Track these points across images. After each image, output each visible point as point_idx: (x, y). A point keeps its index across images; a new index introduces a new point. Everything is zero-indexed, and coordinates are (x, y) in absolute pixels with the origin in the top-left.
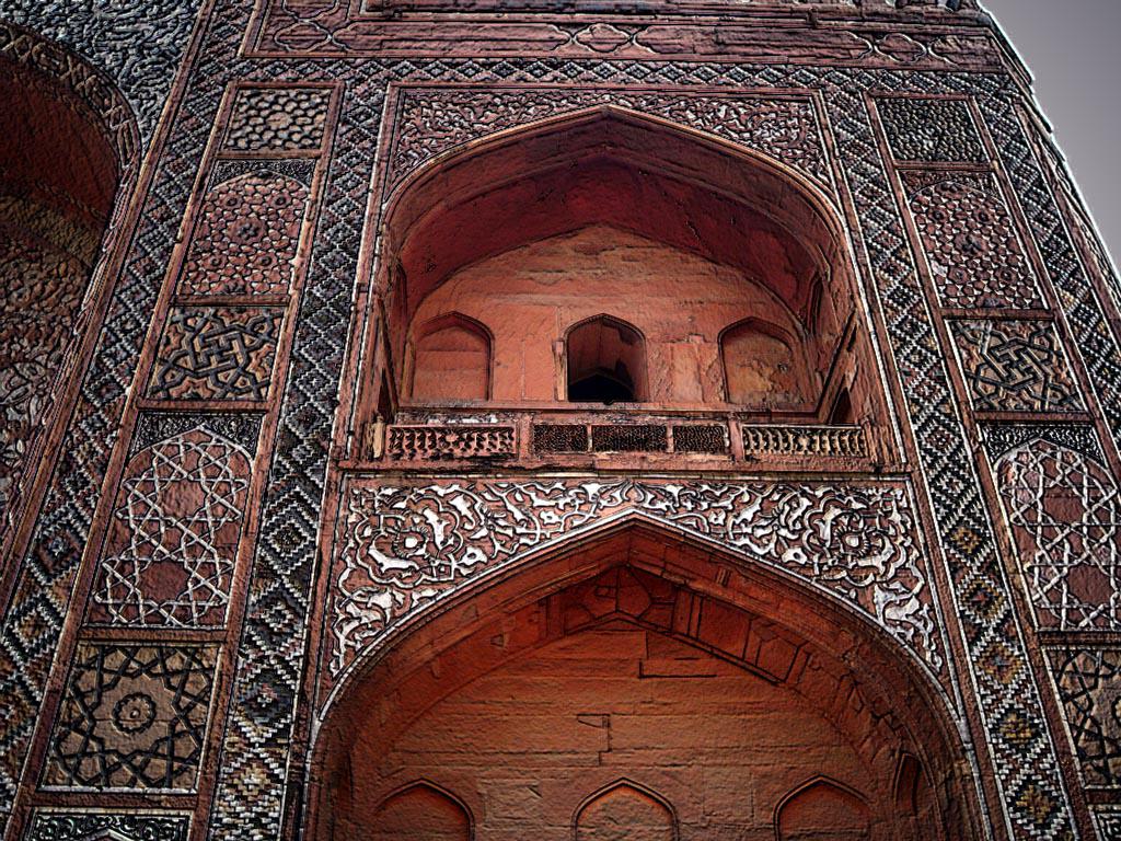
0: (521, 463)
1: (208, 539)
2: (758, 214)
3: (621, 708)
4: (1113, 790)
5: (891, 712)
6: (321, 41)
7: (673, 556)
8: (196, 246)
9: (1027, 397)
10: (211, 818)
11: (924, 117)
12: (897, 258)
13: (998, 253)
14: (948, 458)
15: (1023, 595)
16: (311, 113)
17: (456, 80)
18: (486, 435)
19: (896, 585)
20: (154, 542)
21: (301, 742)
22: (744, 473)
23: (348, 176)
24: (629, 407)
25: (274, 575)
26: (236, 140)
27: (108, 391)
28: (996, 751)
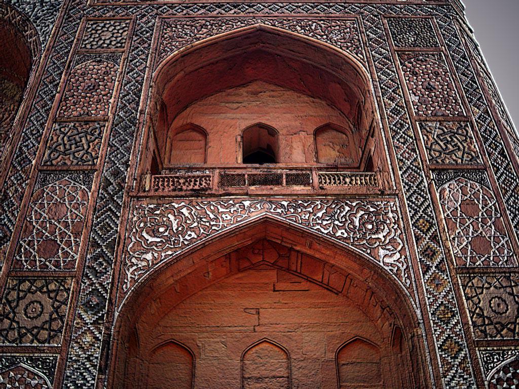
0: (213, 192)
1: (68, 230)
2: (330, 74)
3: (263, 306)
4: (488, 341)
5: (388, 307)
7: (285, 234)
8: (66, 95)
9: (454, 158)
10: (67, 357)
11: (410, 27)
13: (443, 90)
14: (416, 187)
15: (449, 251)
16: (121, 31)
17: (189, 14)
19: (390, 247)
20: (44, 231)
21: (109, 322)
22: (319, 195)
23: (137, 60)
24: (271, 166)
25: (99, 246)
26: (86, 44)
27: (24, 162)
28: (434, 324)
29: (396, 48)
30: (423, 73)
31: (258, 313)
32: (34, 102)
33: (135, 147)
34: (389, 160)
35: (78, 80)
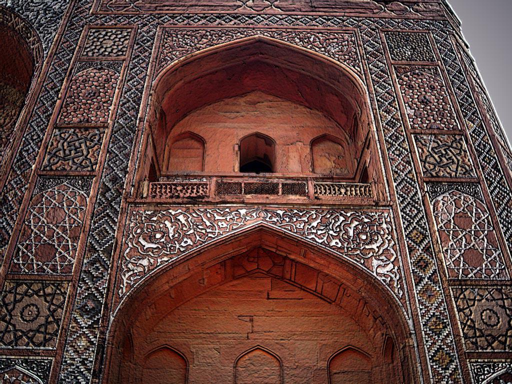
0: (210, 200)
1: (66, 234)
2: (328, 86)
4: (478, 352)
5: (381, 316)
6: (128, 7)
7: (280, 243)
8: (67, 101)
9: (449, 171)
11: (407, 41)
12: (391, 106)
13: (438, 104)
14: (411, 199)
15: (442, 263)
16: (122, 40)
17: (189, 24)
18: (195, 187)
19: (383, 257)
20: (42, 235)
22: (314, 205)
23: (137, 68)
24: (267, 175)
25: (96, 251)
26: (87, 52)
28: (425, 334)
29: (393, 62)
30: (419, 86)
31: (251, 321)
32: (36, 108)
33: (134, 154)
34: (384, 171)
35: (79, 87)
